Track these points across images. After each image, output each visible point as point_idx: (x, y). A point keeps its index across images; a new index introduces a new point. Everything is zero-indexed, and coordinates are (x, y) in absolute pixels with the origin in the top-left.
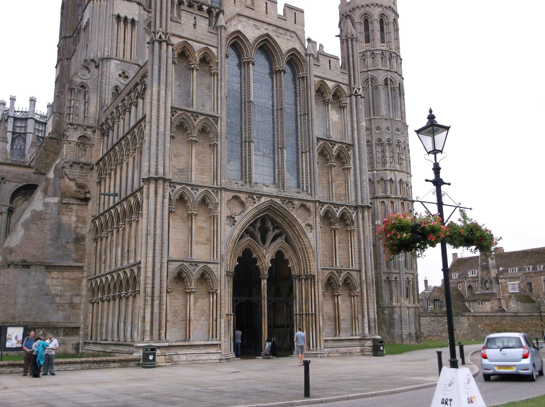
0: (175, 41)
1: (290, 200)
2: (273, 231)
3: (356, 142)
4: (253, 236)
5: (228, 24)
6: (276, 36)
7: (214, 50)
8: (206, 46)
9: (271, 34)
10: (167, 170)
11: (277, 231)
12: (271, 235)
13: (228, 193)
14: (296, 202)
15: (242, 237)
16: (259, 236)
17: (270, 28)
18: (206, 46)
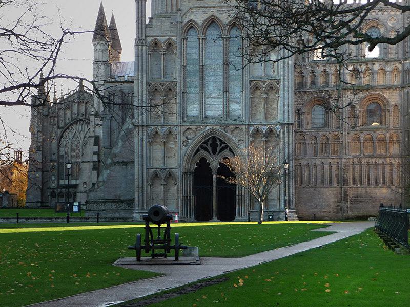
0: (149, 40)
1: (226, 127)
2: (221, 146)
3: (282, 78)
4: (207, 150)
5: (184, 17)
6: (220, 14)
7: (174, 38)
8: (167, 37)
9: (217, 14)
10: (145, 120)
11: (223, 145)
12: (218, 149)
13: (184, 127)
14: (232, 127)
15: (198, 151)
16: (210, 150)
17: (215, 9)
18: (167, 37)
